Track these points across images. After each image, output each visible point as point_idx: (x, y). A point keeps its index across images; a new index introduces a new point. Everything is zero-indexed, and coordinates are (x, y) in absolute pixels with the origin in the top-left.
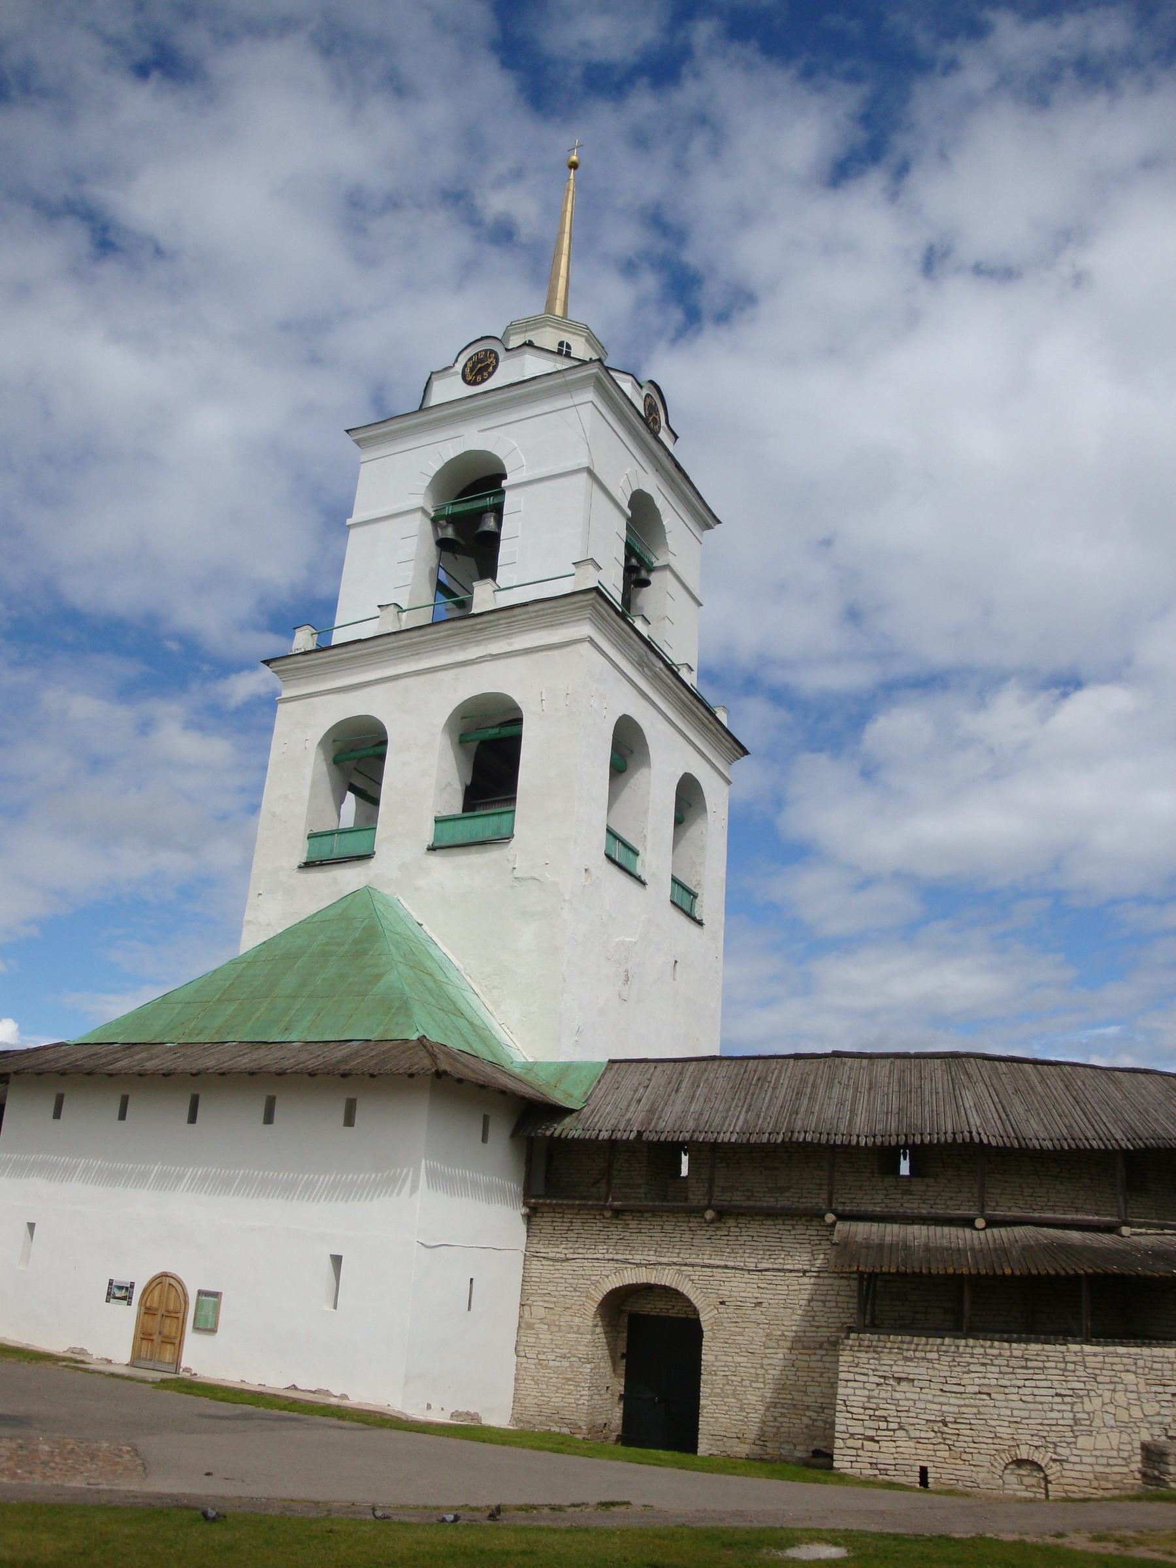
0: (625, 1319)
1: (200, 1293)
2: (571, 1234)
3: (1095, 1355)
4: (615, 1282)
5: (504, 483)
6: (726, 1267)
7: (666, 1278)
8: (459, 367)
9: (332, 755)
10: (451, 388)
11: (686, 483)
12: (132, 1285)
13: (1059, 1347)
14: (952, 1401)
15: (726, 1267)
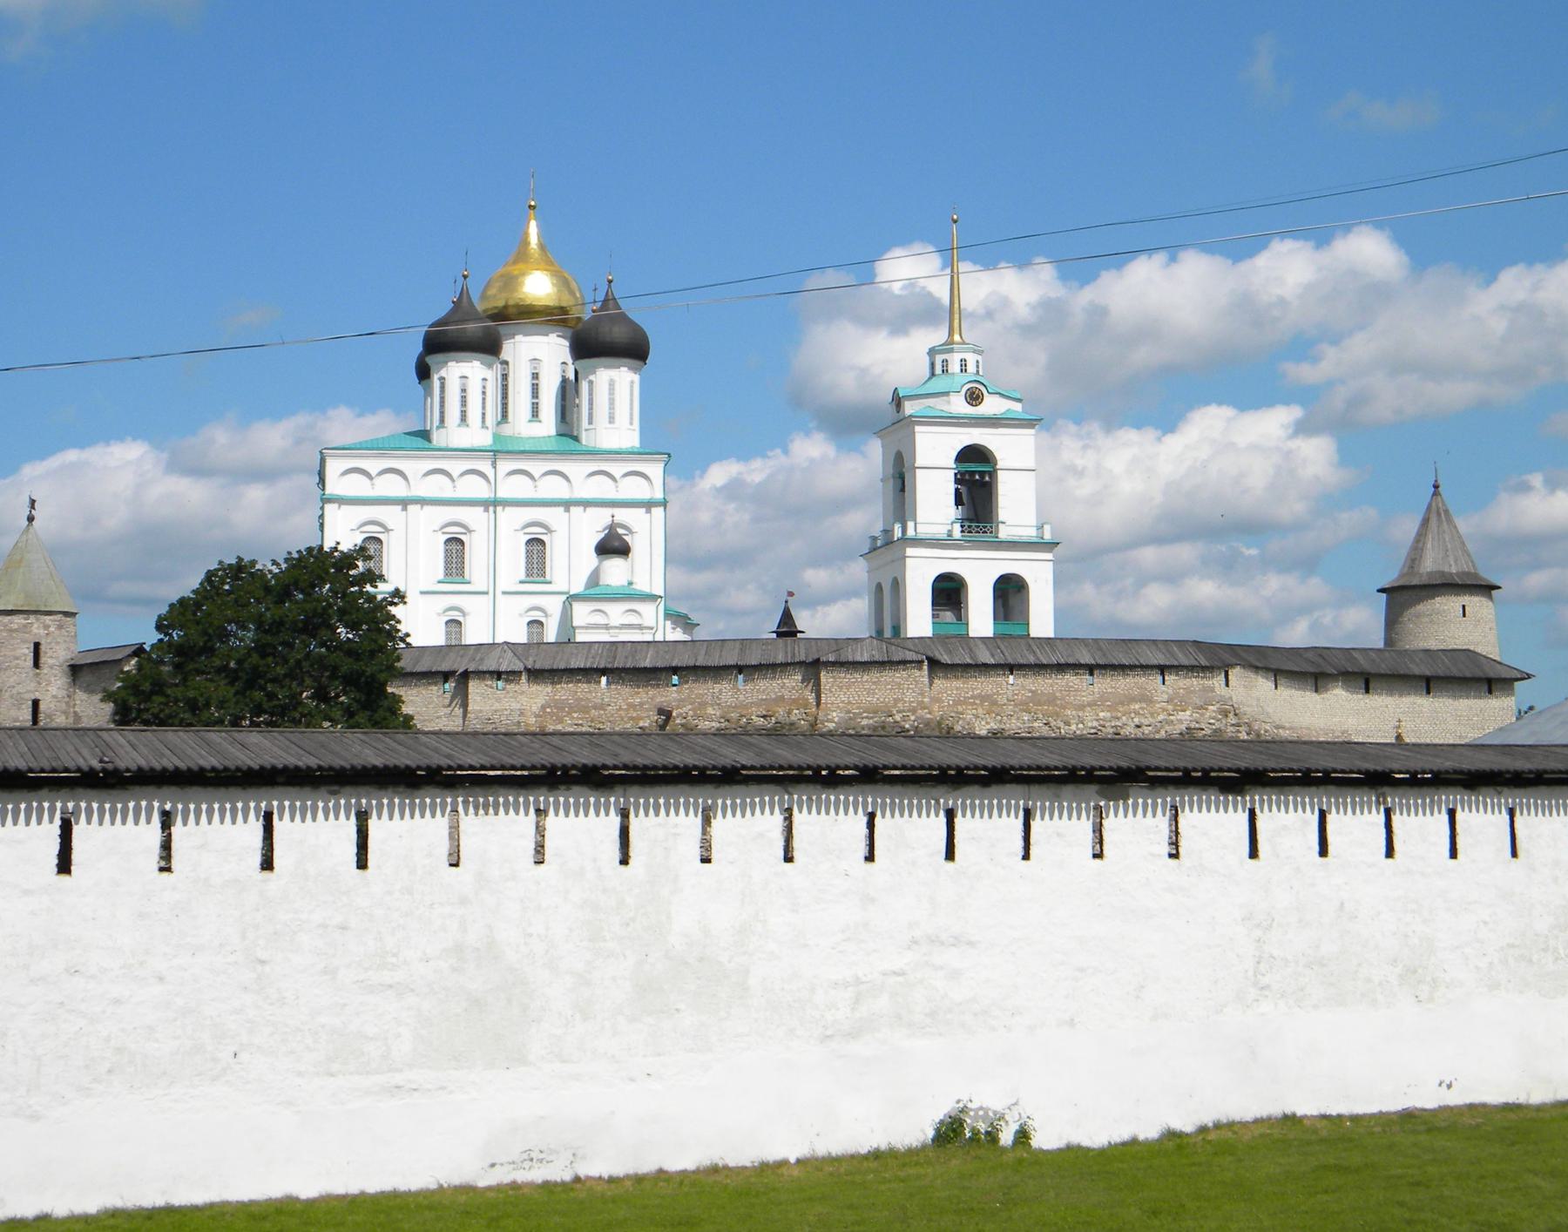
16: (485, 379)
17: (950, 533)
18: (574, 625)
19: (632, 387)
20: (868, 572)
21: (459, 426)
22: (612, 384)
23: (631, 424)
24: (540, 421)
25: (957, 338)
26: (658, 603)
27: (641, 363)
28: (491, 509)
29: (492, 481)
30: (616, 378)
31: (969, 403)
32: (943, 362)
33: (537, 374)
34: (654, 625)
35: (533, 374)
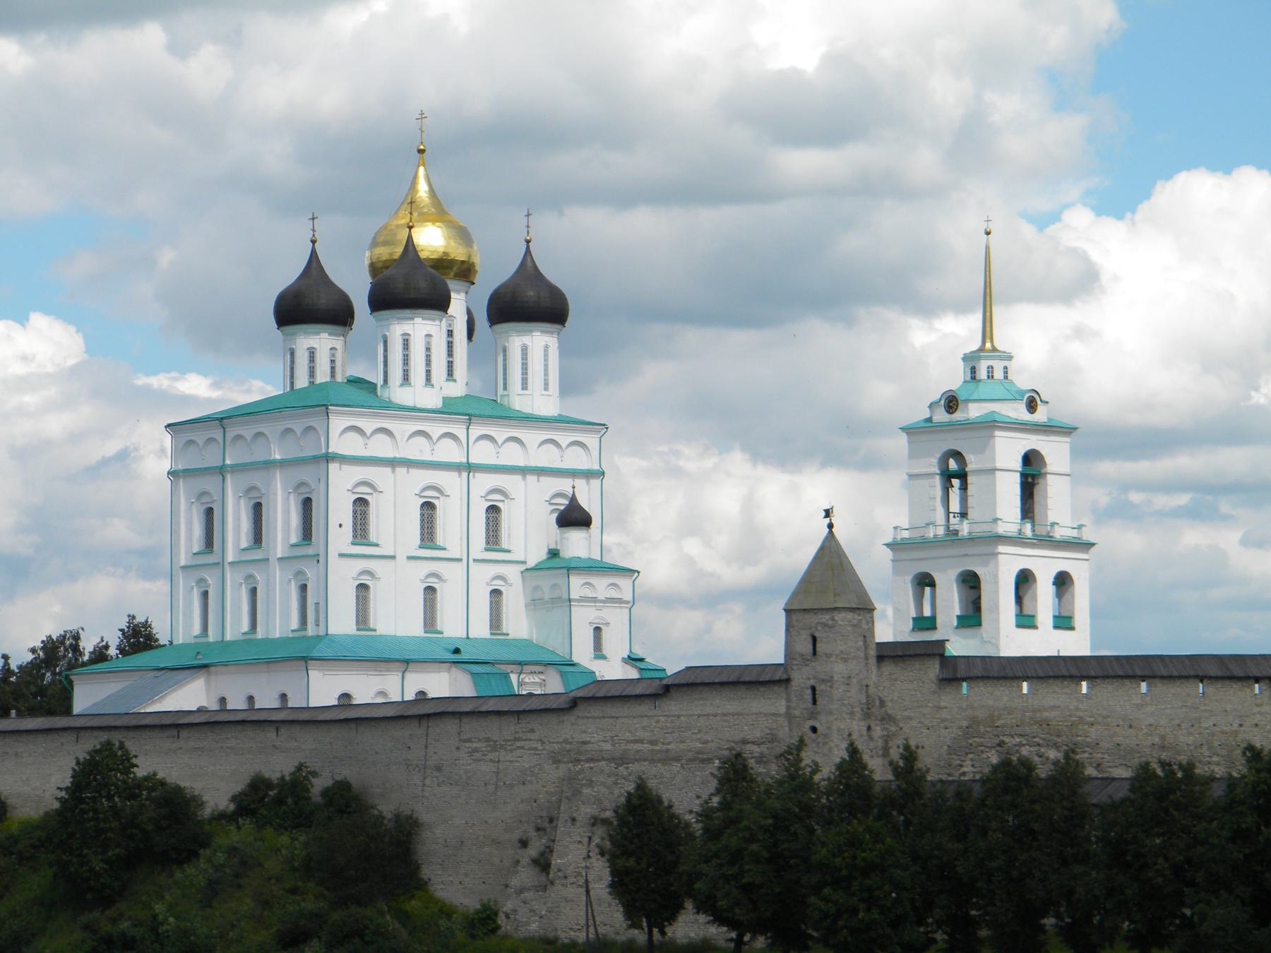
8: (942, 402)
10: (941, 416)
16: (429, 336)
17: (1020, 532)
18: (571, 597)
19: (546, 355)
20: (892, 561)
21: (402, 385)
23: (546, 389)
24: (455, 381)
25: (988, 345)
26: (634, 577)
27: (559, 327)
28: (465, 474)
30: (529, 343)
32: (988, 368)
33: (452, 331)
34: (631, 599)
35: (448, 330)
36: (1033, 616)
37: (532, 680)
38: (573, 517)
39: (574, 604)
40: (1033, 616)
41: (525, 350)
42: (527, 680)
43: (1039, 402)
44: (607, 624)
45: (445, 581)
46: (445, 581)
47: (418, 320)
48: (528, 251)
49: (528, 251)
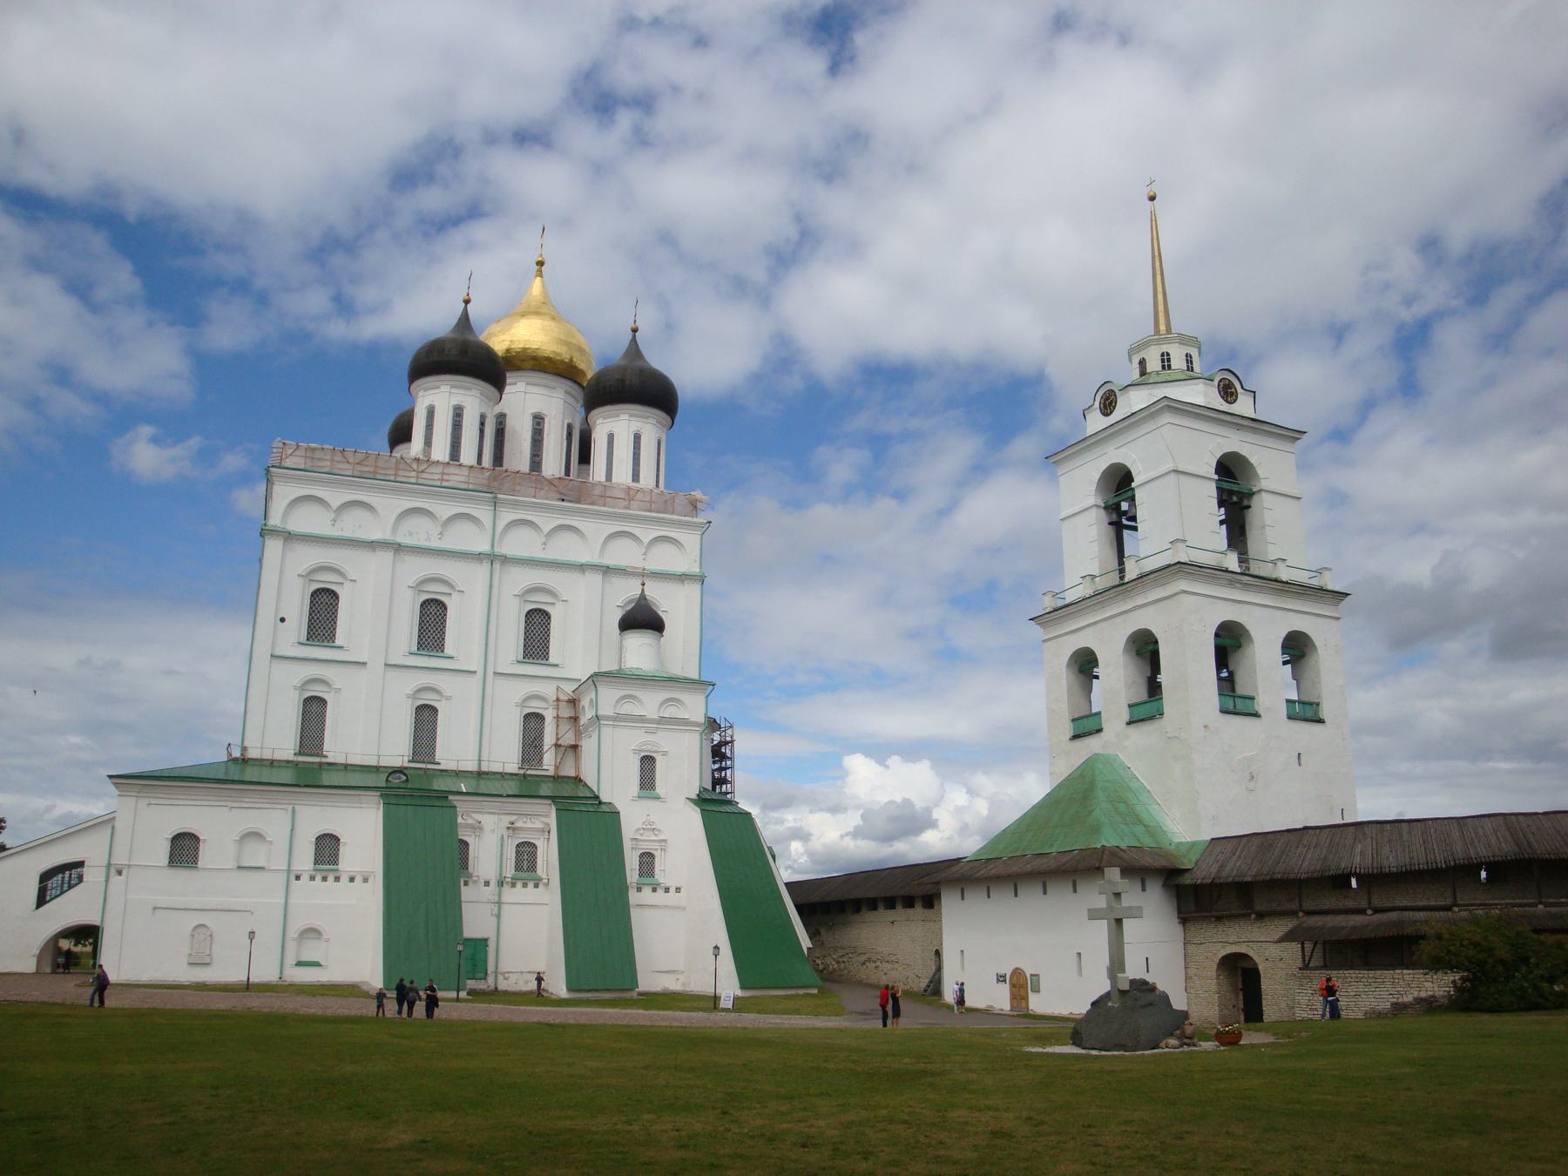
0: (1239, 972)
1: (1031, 975)
2: (1203, 930)
3: (1409, 974)
4: (1223, 953)
5: (1133, 485)
6: (1267, 942)
7: (1242, 949)
8: (1097, 404)
9: (1077, 669)
10: (1096, 422)
11: (1265, 425)
12: (1005, 976)
13: (1391, 972)
14: (1345, 1000)
15: (1267, 942)
22: (637, 438)
26: (707, 693)
29: (490, 531)
31: (1223, 398)
32: (1163, 355)
36: (1252, 698)
37: (530, 825)
38: (643, 619)
39: (607, 722)
40: (1252, 698)
41: (611, 437)
42: (518, 824)
43: (1239, 389)
44: (665, 754)
45: (449, 698)
46: (449, 698)
47: (445, 388)
48: (634, 339)
49: (634, 339)
